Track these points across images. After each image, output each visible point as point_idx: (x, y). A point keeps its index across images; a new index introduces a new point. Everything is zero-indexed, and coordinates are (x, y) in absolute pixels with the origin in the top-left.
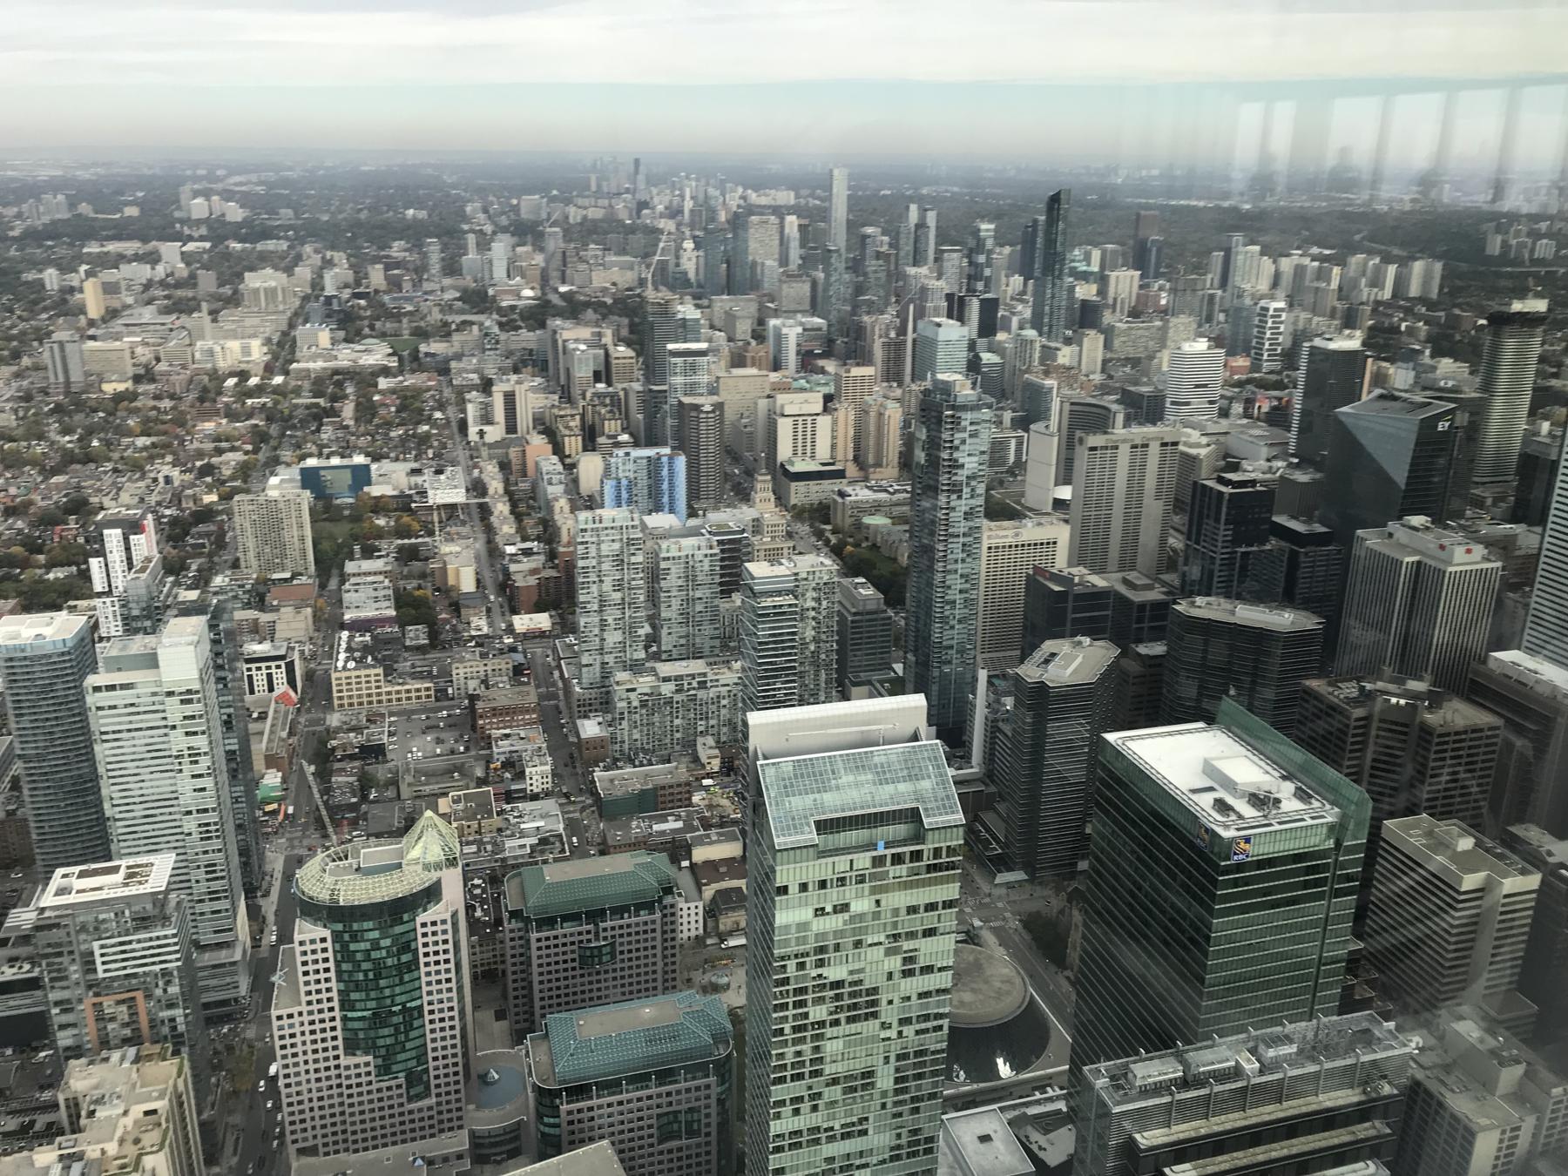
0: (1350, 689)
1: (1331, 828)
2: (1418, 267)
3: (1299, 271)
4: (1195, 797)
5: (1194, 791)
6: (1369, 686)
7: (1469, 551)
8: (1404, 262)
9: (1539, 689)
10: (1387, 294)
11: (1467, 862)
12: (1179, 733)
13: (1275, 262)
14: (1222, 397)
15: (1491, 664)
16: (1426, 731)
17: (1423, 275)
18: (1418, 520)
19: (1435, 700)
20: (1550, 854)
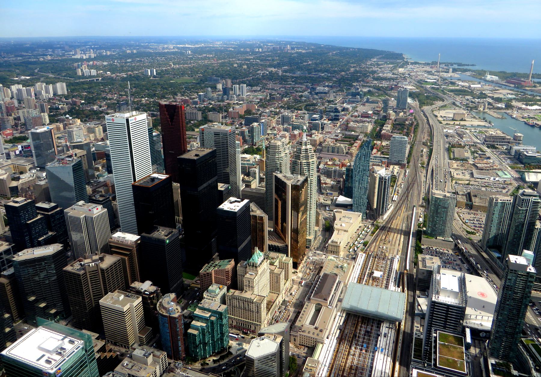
0: (77, 266)
1: (83, 348)
2: (58, 85)
3: (19, 90)
4: (38, 362)
5: (38, 360)
6: (82, 263)
7: (97, 209)
8: (54, 83)
9: (126, 242)
10: (51, 95)
11: (123, 304)
12: (27, 337)
13: (9, 88)
14: (5, 149)
15: (113, 239)
16: (102, 270)
17: (61, 88)
18: (81, 203)
19: (102, 259)
20: (142, 289)
